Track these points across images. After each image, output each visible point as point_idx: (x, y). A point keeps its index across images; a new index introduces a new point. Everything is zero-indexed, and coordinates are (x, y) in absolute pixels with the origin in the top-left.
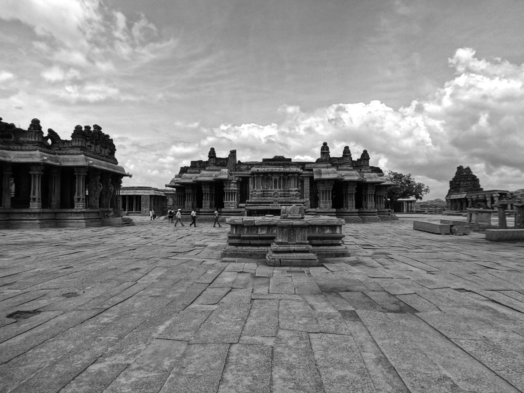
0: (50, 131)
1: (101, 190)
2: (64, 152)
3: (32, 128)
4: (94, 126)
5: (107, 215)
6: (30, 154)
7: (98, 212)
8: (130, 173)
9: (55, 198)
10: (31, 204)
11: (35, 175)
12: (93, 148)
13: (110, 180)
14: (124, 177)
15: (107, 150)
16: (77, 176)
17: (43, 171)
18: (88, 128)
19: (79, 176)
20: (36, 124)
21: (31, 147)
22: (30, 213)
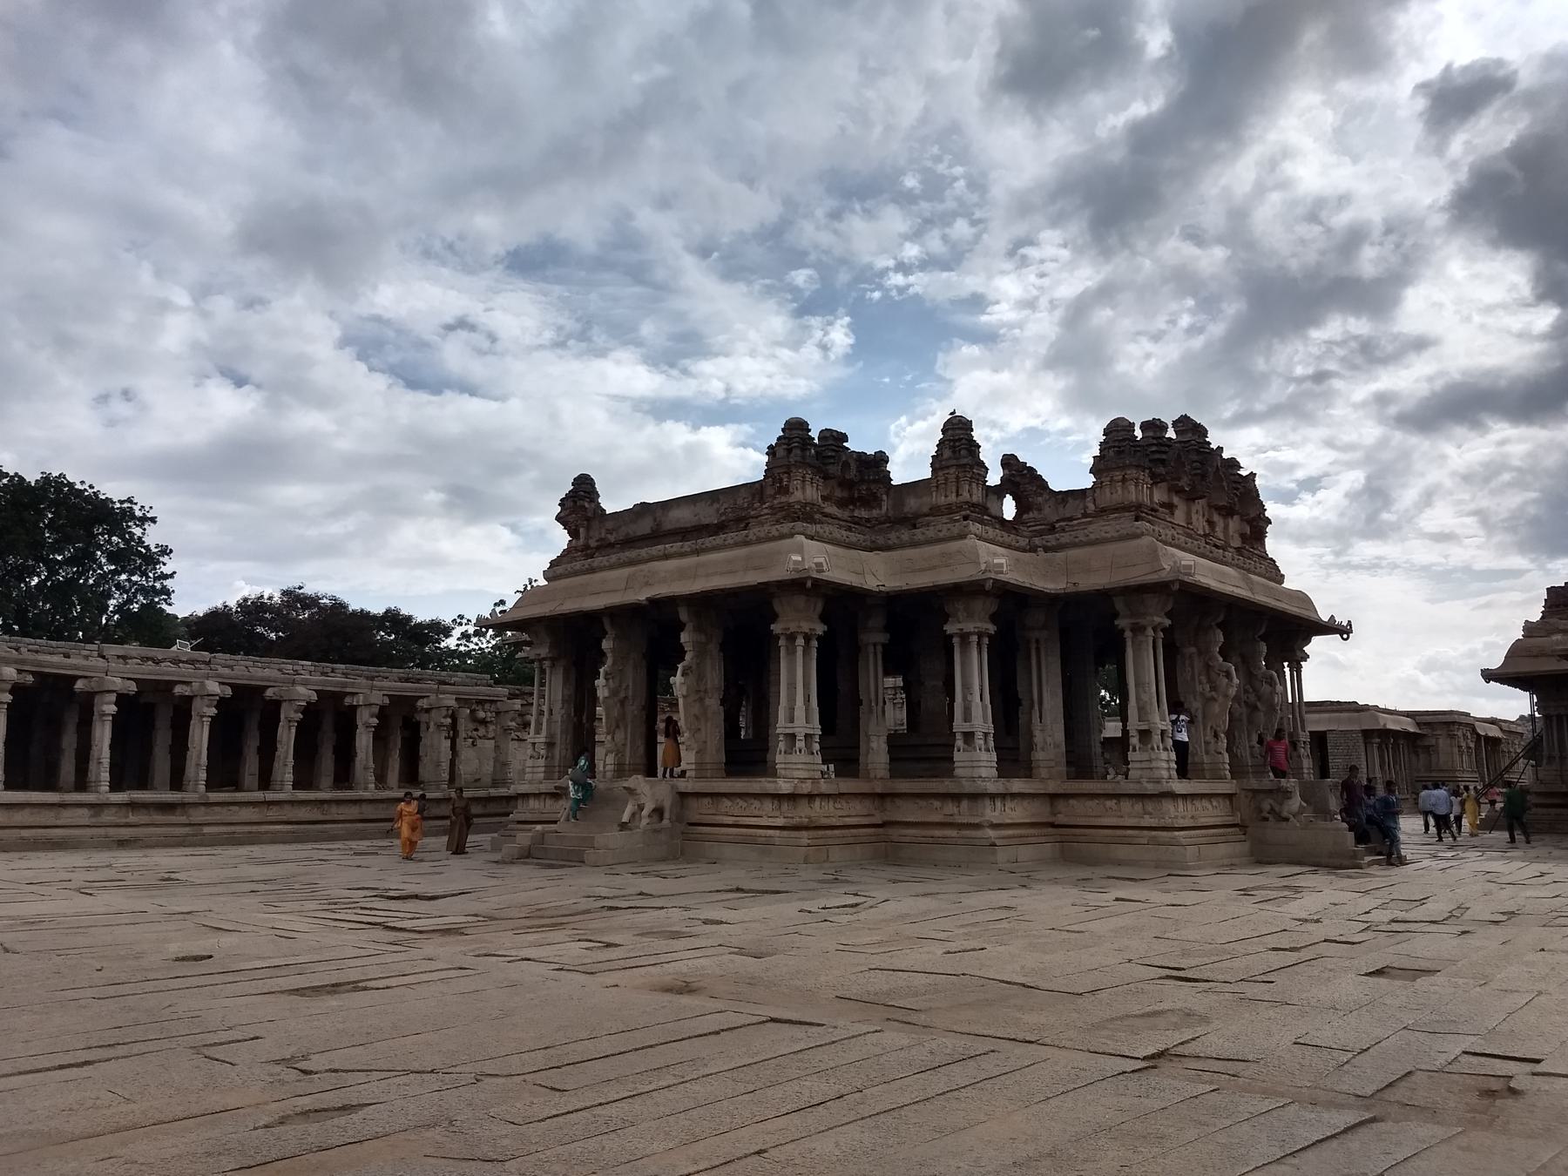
0: (1009, 462)
1: (1232, 692)
2: (1065, 538)
3: (947, 453)
4: (1175, 423)
5: (1272, 811)
6: (943, 554)
7: (1229, 796)
8: (1341, 619)
9: (1048, 732)
10: (957, 756)
11: (965, 637)
12: (1179, 516)
13: (1264, 648)
14: (1315, 639)
15: (1234, 524)
16: (1128, 634)
17: (993, 618)
18: (1153, 426)
19: (1138, 630)
20: (958, 440)
21: (942, 526)
22: (956, 797)
